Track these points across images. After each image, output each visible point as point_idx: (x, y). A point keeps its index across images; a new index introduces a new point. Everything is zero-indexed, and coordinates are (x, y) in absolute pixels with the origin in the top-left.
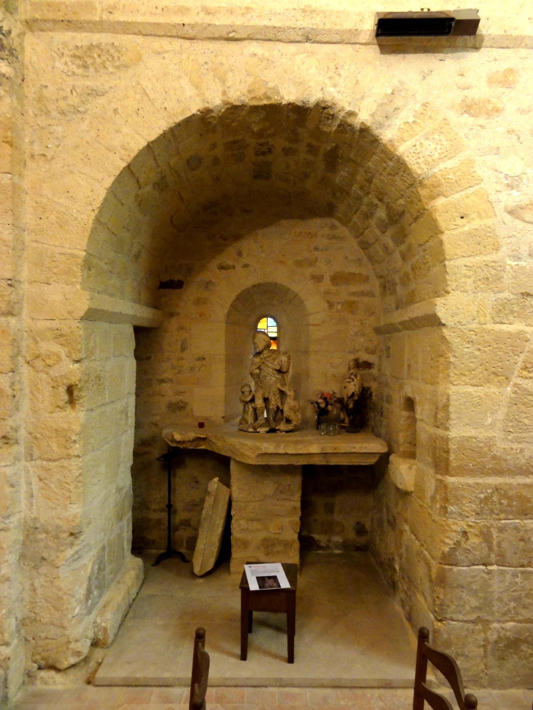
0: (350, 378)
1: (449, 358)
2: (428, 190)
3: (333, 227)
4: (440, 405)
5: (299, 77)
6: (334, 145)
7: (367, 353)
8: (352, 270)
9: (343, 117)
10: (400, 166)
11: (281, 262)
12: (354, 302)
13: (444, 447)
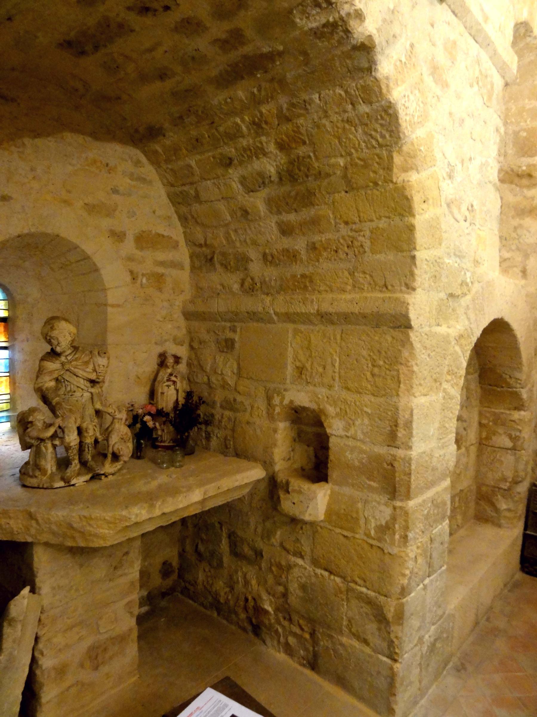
0: (169, 380)
1: (412, 366)
2: (402, 158)
3: (137, 163)
4: (401, 422)
6: (281, 48)
7: (176, 344)
8: (162, 229)
9: (349, 14)
11: (66, 202)
12: (162, 275)
13: (407, 469)
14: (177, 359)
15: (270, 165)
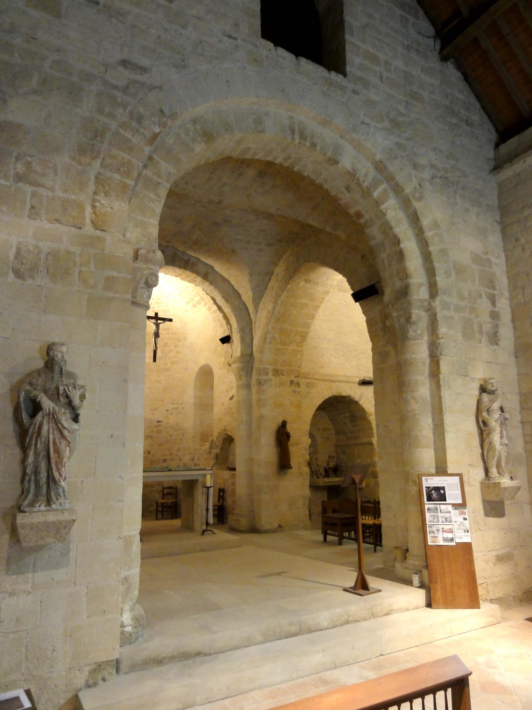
5: (346, 390)
10: (363, 409)
14: (333, 457)
15: (348, 414)
